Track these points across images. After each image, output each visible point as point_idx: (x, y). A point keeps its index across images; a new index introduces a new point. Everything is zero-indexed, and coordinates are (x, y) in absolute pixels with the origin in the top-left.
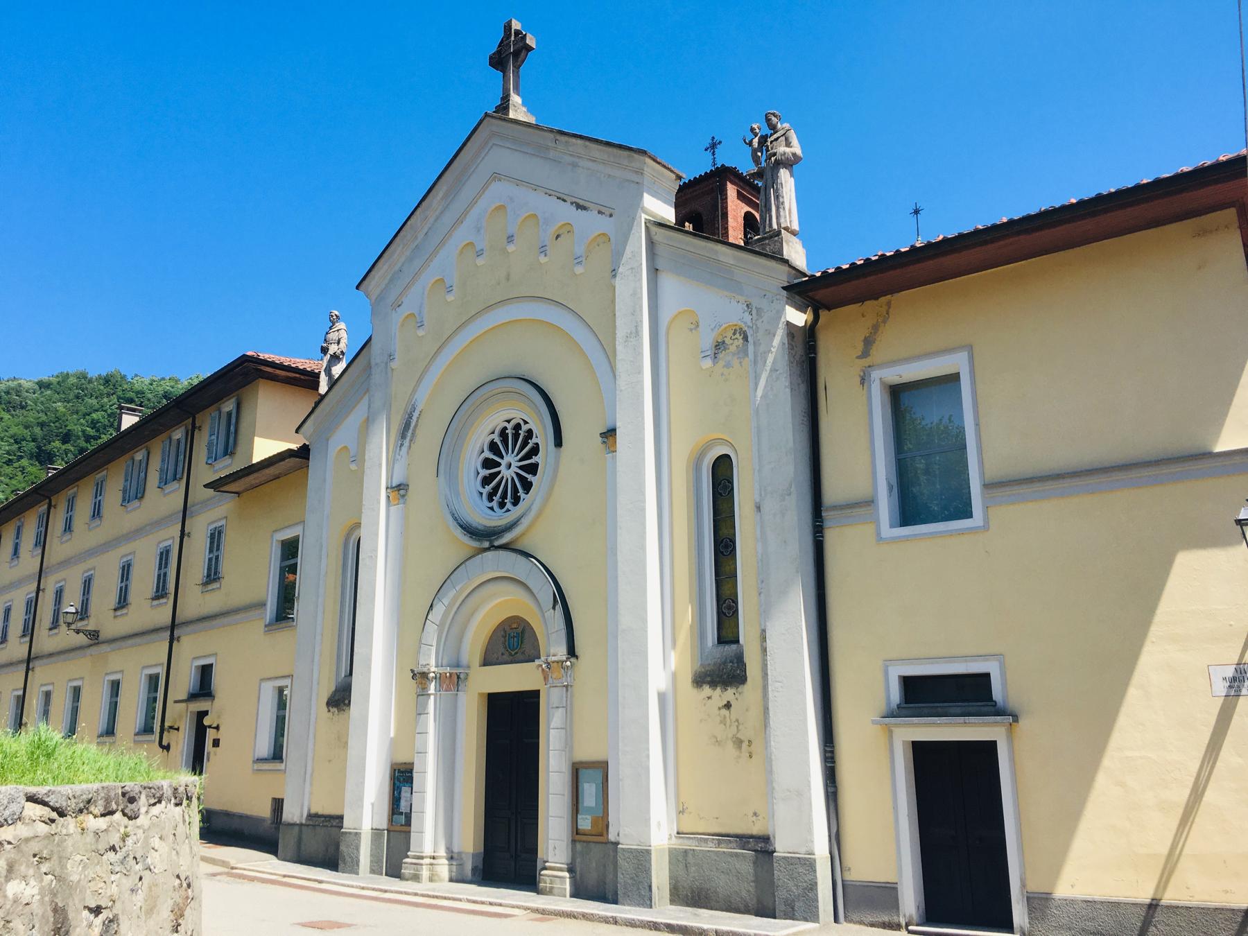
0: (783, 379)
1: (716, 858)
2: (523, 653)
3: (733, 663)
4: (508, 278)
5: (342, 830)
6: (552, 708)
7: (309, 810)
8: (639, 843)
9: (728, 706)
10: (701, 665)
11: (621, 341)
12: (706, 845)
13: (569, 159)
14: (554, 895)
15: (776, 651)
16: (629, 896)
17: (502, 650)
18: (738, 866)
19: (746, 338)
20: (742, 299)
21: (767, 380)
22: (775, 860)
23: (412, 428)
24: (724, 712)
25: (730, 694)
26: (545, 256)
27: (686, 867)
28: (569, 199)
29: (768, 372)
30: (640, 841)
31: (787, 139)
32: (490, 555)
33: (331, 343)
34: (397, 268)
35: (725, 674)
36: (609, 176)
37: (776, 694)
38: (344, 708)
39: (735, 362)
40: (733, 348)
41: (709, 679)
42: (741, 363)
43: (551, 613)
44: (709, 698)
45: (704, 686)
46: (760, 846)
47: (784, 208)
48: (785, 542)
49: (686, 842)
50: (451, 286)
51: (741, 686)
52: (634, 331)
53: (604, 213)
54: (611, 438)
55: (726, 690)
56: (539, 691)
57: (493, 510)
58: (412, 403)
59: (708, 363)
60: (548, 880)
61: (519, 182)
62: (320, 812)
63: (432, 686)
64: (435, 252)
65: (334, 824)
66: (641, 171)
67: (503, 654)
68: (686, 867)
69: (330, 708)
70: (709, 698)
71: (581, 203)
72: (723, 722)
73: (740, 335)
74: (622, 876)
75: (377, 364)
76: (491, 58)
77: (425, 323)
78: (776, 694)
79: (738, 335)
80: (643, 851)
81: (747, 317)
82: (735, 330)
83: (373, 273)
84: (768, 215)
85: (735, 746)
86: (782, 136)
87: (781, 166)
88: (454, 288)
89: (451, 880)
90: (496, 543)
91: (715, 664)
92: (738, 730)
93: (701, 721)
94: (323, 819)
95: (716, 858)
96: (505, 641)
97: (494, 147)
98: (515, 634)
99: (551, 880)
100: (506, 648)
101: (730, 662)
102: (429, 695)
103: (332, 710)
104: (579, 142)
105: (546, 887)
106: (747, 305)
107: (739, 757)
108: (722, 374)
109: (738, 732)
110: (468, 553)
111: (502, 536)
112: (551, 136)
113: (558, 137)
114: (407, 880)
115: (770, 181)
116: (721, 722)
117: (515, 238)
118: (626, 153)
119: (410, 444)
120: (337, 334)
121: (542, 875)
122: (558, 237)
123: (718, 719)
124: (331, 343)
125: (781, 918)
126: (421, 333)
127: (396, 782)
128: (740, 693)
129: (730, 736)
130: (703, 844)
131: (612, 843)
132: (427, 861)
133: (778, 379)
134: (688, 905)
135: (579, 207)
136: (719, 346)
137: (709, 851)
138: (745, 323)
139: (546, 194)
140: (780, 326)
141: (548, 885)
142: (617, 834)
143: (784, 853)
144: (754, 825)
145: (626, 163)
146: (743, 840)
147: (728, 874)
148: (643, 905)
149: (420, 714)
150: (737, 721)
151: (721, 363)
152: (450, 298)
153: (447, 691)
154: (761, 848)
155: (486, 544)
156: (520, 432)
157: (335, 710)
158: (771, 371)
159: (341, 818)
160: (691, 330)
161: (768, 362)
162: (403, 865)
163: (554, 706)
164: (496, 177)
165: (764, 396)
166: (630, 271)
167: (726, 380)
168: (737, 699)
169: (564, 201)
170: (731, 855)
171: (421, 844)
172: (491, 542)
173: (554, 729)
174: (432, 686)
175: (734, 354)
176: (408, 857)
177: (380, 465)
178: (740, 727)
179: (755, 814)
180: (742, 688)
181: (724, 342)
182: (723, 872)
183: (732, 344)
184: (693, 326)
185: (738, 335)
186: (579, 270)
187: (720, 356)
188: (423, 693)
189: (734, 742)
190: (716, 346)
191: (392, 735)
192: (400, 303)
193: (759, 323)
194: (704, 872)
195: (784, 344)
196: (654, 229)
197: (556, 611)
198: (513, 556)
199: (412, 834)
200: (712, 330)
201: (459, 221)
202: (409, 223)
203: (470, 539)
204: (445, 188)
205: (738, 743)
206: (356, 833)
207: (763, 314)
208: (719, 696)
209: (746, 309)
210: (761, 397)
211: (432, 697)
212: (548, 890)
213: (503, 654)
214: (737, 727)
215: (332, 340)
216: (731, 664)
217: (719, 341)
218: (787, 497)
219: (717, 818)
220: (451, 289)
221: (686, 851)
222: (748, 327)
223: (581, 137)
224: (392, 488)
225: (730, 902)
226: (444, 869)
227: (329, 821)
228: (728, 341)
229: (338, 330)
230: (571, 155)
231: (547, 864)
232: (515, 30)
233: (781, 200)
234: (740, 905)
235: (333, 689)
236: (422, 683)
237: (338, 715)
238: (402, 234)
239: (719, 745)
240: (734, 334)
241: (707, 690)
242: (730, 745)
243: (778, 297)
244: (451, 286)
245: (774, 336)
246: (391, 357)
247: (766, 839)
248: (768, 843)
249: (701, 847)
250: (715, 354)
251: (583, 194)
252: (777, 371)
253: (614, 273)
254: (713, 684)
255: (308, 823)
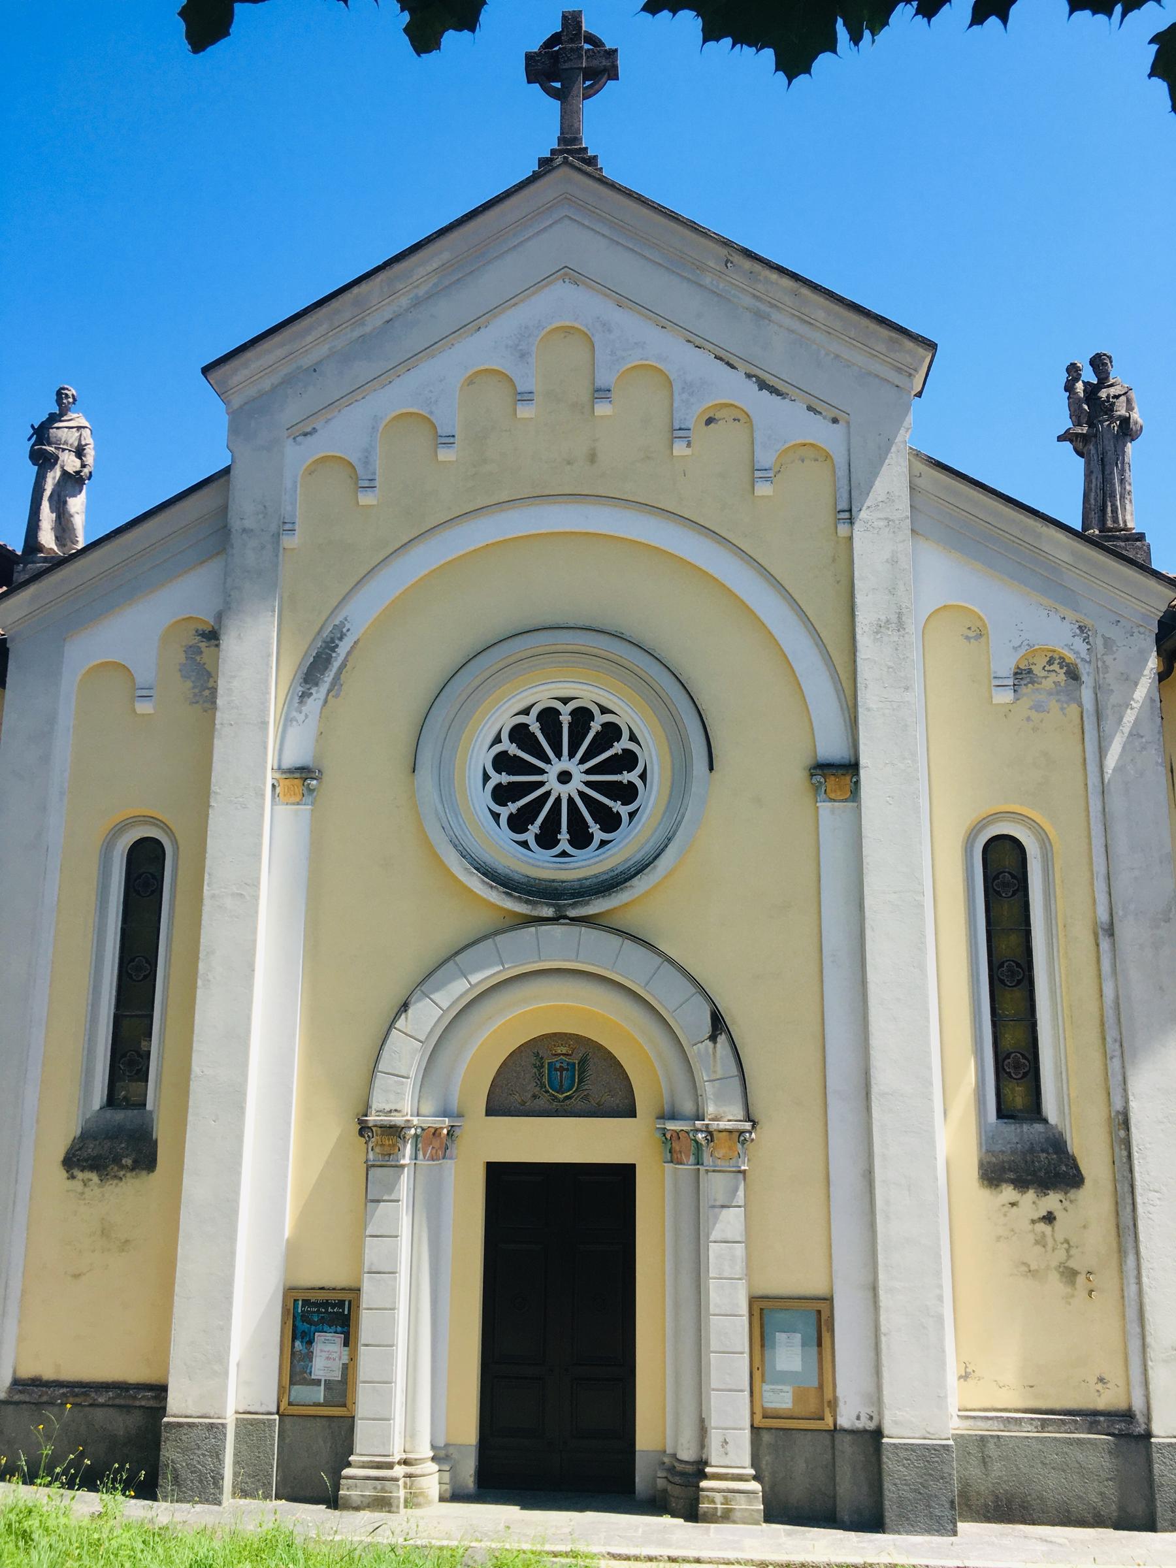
0: (1154, 752)
1: (1040, 1447)
2: (586, 1098)
3: (1048, 1153)
4: (592, 458)
5: (165, 1419)
6: (713, 1207)
7: (15, 1372)
8: (928, 1435)
9: (1049, 1218)
10: (988, 1151)
11: (866, 629)
12: (1017, 1428)
13: (748, 301)
14: (734, 1522)
15: (1148, 1146)
16: (908, 1519)
17: (532, 1088)
18: (1080, 1457)
19: (1073, 675)
20: (1070, 615)
21: (1124, 748)
22: (1154, 1449)
23: (336, 664)
24: (1042, 1227)
25: (1052, 1201)
26: (689, 445)
27: (985, 1463)
28: (743, 368)
29: (1126, 735)
30: (929, 1433)
31: (1129, 401)
32: (557, 931)
33: (64, 450)
34: (307, 361)
35: (1040, 1170)
36: (837, 356)
37: (1151, 1209)
38: (122, 1173)
39: (1053, 705)
40: (1048, 684)
41: (1012, 1176)
42: (1062, 709)
43: (707, 1047)
44: (1013, 1204)
45: (1004, 1186)
46: (1119, 1427)
47: (1131, 501)
48: (1161, 988)
49: (981, 1424)
50: (453, 436)
51: (1073, 1191)
52: (894, 618)
53: (820, 413)
54: (833, 778)
55: (1046, 1194)
56: (633, 1166)
57: (530, 850)
58: (337, 622)
59: (1006, 696)
60: (718, 1497)
61: (623, 301)
62: (48, 1374)
63: (409, 1149)
64: (410, 362)
65: (101, 1400)
66: (912, 371)
67: (535, 1096)
68: (985, 1463)
69: (76, 1172)
70: (1013, 1204)
71: (772, 381)
72: (1041, 1241)
73: (1061, 668)
74: (893, 1488)
75: (244, 530)
76: (530, 58)
77: (377, 483)
78: (1151, 1209)
79: (1056, 667)
80: (936, 1448)
81: (1082, 647)
82: (1051, 658)
83: (249, 354)
84: (1109, 504)
85: (1064, 1280)
86: (1123, 394)
87: (1129, 438)
88: (456, 440)
89: (442, 1499)
90: (572, 913)
91: (1014, 1152)
92: (1069, 1257)
93: (999, 1238)
94: (64, 1390)
95: (1040, 1447)
96: (541, 1074)
97: (567, 222)
98: (565, 1065)
99: (725, 1498)
100: (542, 1086)
101: (1043, 1151)
102: (403, 1166)
103: (80, 1175)
104: (786, 282)
105: (717, 1508)
106: (1080, 627)
107: (1073, 1296)
108: (1028, 719)
109: (1069, 1257)
110: (479, 921)
111: (587, 903)
112: (723, 252)
113: (738, 259)
114: (357, 1509)
115: (1110, 455)
116: (1037, 1242)
117: (613, 395)
118: (885, 332)
119: (328, 695)
120: (77, 434)
121: (703, 1490)
122: (709, 421)
123: (1031, 1238)
124: (64, 450)
125: (1165, 1530)
126: (366, 499)
127: (299, 1324)
128: (1071, 1201)
129: (1054, 1264)
130: (1012, 1427)
131: (845, 1431)
132: (399, 1471)
133: (1143, 748)
134: (988, 1520)
135: (763, 385)
136: (1022, 676)
137: (1027, 1437)
138: (1077, 653)
139: (689, 341)
140: (1146, 672)
141: (719, 1506)
142: (855, 1417)
143: (1168, 1437)
144: (1100, 1396)
145: (881, 347)
146: (1091, 1418)
147: (1064, 1471)
148: (937, 1531)
149: (378, 1201)
150: (1067, 1241)
151: (1026, 703)
152: (445, 455)
153: (433, 1160)
154: (1120, 1430)
155: (548, 912)
156: (592, 724)
157: (94, 1177)
158: (1131, 734)
159: (160, 1390)
160: (967, 638)
161: (1125, 720)
162: (343, 1482)
163: (718, 1203)
164: (571, 275)
165: (1119, 769)
166: (885, 523)
167: (1035, 729)
168: (1066, 1210)
169: (733, 367)
170: (1069, 1442)
171: (387, 1438)
172: (558, 908)
173: (715, 1242)
174: (409, 1149)
175: (1050, 694)
176: (349, 1465)
177: (264, 724)
178: (1073, 1251)
179: (1101, 1380)
180: (1073, 1194)
181: (1030, 671)
182: (1053, 1468)
183: (1046, 677)
184: (971, 634)
185: (1056, 667)
186: (763, 489)
187: (1024, 690)
188: (387, 1161)
189: (1062, 1274)
190: (1016, 674)
191: (287, 1234)
192: (309, 429)
193: (1108, 659)
194: (1018, 1469)
195: (1152, 700)
196: (921, 467)
197: (718, 1045)
198: (615, 941)
199: (360, 1425)
200: (1015, 648)
201: (475, 324)
202: (355, 290)
203: (504, 896)
204: (446, 256)
205: (1070, 1275)
206: (212, 1425)
207: (1114, 649)
208: (1031, 1203)
209: (1078, 631)
210: (1114, 770)
211: (406, 1169)
212: (719, 1514)
213: (535, 1096)
214: (1067, 1251)
215: (66, 443)
216: (1045, 1155)
217: (1022, 667)
218: (1162, 924)
219: (1032, 1387)
220: (452, 440)
221: (982, 1438)
222: (1083, 660)
223: (795, 277)
224: (284, 772)
225: (1068, 1511)
226: (432, 1481)
227: (85, 1394)
228: (1037, 670)
229: (79, 428)
230: (754, 296)
231: (708, 1470)
232: (585, 31)
233: (1128, 488)
234: (1086, 1515)
235: (75, 1130)
236: (382, 1145)
237: (100, 1186)
238: (335, 304)
239: (1033, 1276)
240: (1050, 662)
241: (1009, 1193)
242: (1054, 1278)
243: (1142, 630)
244: (453, 436)
245: (1136, 684)
246: (287, 526)
247: (1128, 1415)
248: (1132, 1423)
249: (1008, 1431)
250: (1014, 685)
251: (777, 366)
252: (1142, 737)
253: (849, 515)
254: (1021, 1184)
255: (17, 1398)
